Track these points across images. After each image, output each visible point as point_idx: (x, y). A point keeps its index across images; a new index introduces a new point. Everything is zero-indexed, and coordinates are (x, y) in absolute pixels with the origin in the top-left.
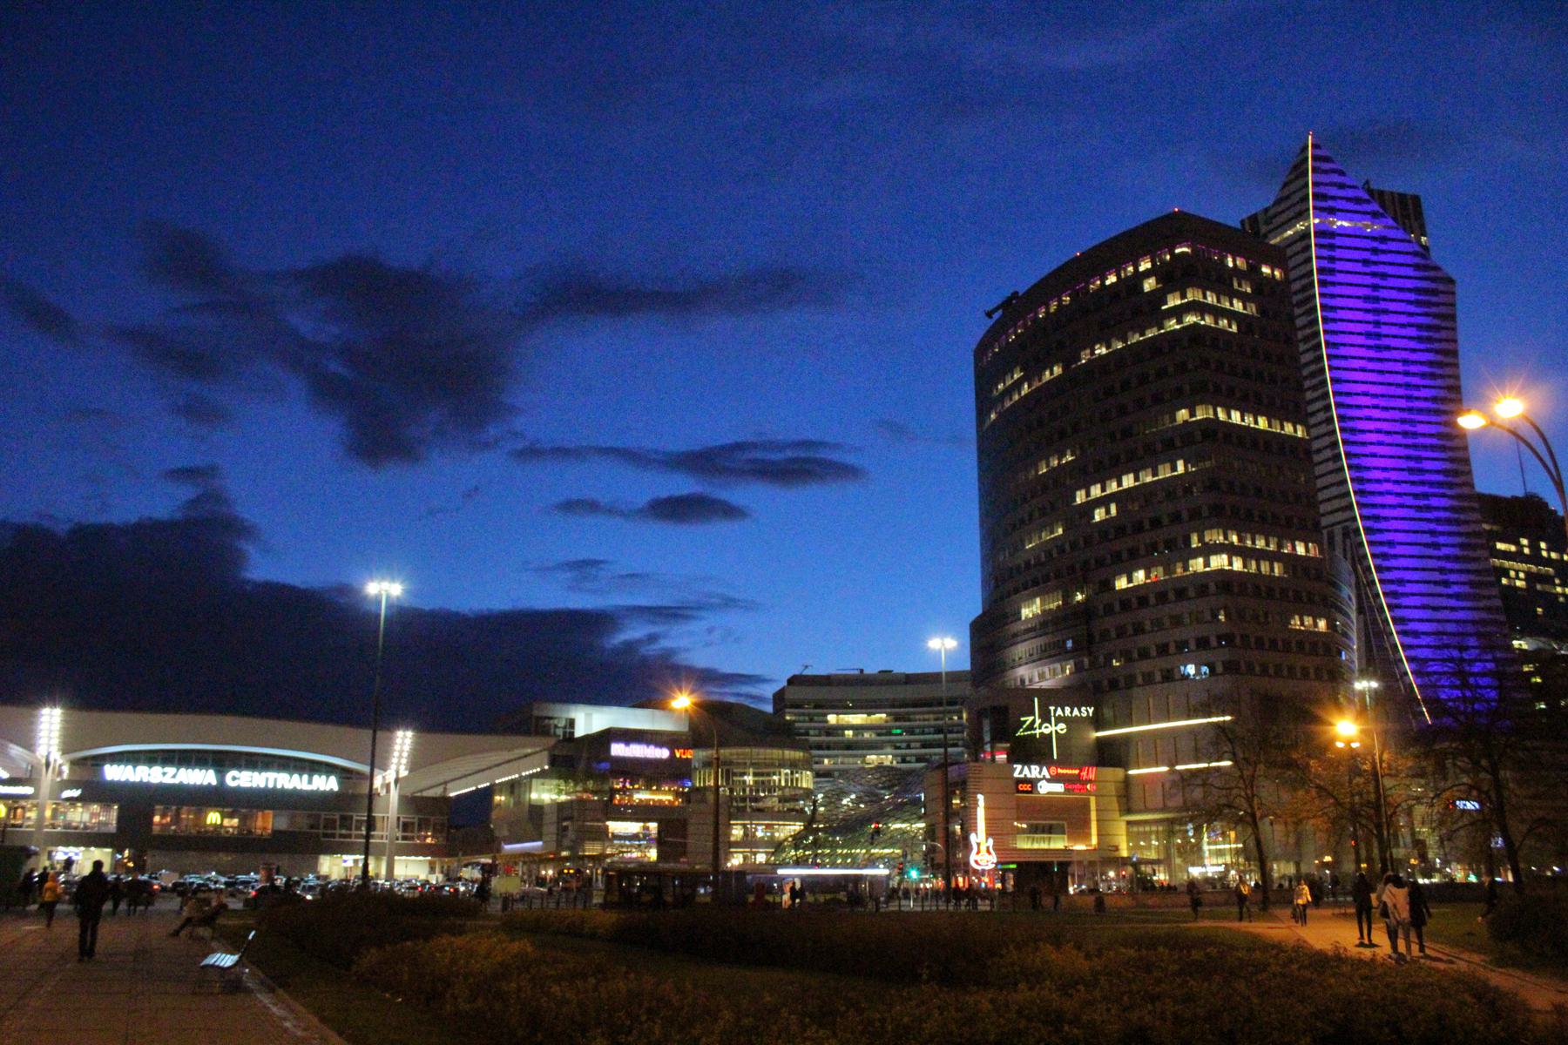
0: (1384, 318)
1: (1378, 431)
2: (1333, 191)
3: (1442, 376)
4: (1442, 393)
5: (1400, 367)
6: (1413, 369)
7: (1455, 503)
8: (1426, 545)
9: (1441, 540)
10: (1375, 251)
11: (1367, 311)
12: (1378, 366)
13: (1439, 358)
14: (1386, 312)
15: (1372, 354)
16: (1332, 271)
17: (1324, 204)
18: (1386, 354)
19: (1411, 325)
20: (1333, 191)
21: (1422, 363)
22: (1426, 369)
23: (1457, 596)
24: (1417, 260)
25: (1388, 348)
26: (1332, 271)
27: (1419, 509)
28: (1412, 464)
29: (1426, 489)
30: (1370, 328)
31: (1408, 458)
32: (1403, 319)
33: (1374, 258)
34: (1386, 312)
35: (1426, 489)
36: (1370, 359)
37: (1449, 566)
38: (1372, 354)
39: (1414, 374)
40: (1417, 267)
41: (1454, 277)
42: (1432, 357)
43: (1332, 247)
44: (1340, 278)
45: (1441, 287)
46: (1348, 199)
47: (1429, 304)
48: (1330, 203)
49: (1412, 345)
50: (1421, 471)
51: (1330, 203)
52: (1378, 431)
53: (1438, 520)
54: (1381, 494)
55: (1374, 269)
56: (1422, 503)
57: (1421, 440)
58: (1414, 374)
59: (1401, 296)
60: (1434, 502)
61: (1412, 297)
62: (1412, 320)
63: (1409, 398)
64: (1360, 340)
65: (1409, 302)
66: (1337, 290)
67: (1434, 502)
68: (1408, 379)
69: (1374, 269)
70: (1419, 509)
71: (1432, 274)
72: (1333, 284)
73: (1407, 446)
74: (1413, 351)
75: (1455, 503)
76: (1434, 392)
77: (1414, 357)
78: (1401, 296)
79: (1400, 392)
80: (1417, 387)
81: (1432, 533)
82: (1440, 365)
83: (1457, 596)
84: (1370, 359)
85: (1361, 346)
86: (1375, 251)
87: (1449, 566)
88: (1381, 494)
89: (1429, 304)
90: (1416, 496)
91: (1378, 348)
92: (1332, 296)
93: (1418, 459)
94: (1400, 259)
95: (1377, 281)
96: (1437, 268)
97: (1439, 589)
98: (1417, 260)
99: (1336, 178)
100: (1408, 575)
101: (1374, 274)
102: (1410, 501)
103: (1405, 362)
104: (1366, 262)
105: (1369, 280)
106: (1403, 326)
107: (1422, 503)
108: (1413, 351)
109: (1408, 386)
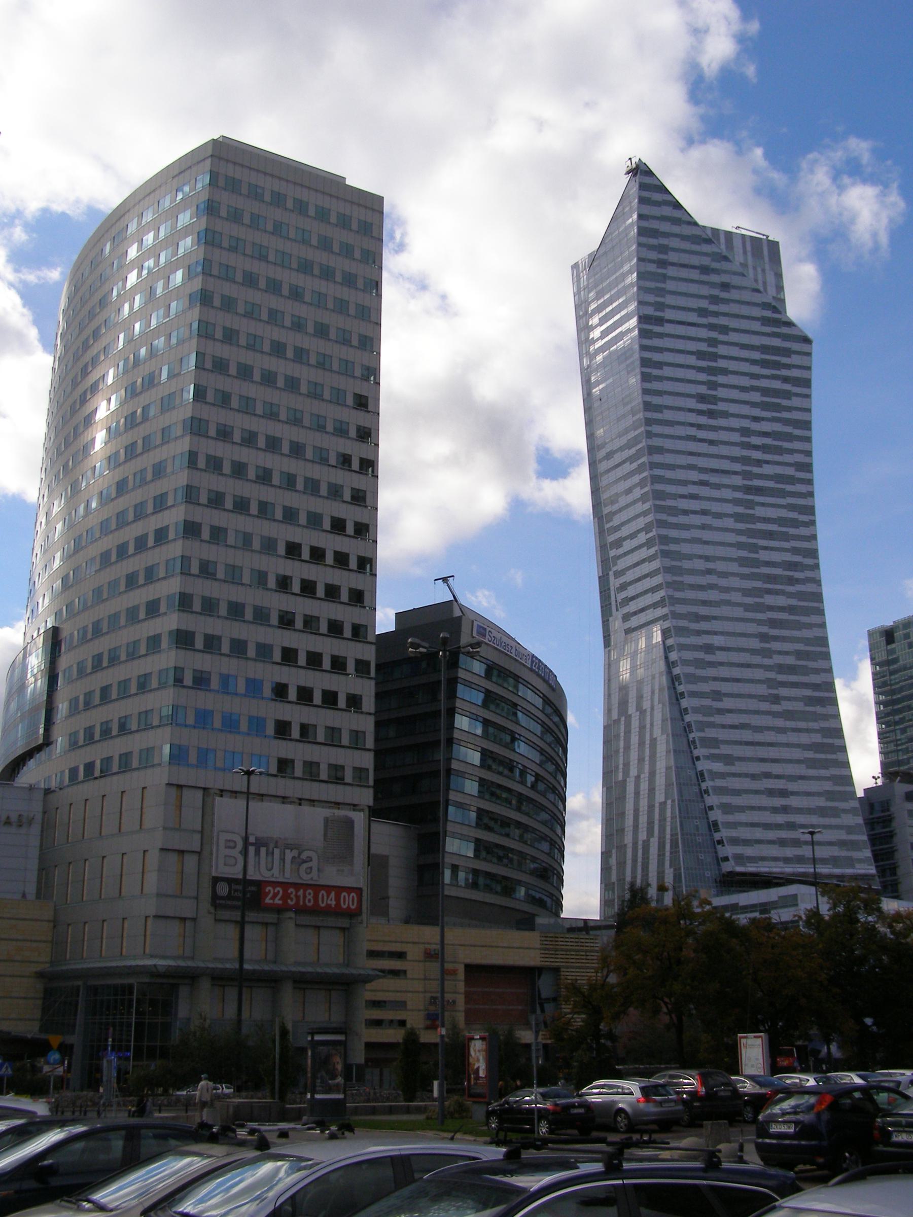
0: (721, 379)
1: (704, 512)
2: (665, 227)
3: (791, 452)
4: (790, 471)
5: (736, 437)
6: (756, 440)
7: (793, 602)
8: (753, 652)
9: (776, 646)
10: (715, 300)
11: (700, 369)
12: (711, 435)
13: (788, 429)
14: (725, 372)
15: (703, 420)
16: (660, 321)
17: (653, 241)
18: (722, 422)
20: (665, 227)
21: (766, 434)
22: (768, 441)
23: (789, 715)
24: (768, 314)
25: (725, 414)
26: (660, 321)
27: (747, 608)
29: (758, 584)
30: (703, 389)
31: (740, 546)
32: (745, 382)
33: (713, 308)
34: (725, 372)
35: (758, 584)
36: (700, 427)
37: (781, 678)
39: (756, 447)
40: (765, 321)
41: (810, 335)
42: (778, 427)
43: (662, 292)
44: (668, 328)
45: (796, 346)
46: (684, 238)
47: (777, 365)
48: (663, 241)
49: (757, 412)
50: (757, 563)
51: (663, 241)
52: (704, 512)
53: (773, 623)
54: (701, 588)
55: (712, 320)
56: (749, 600)
57: (760, 526)
58: (756, 447)
59: (745, 354)
60: (769, 600)
61: (756, 355)
62: (755, 383)
63: (747, 475)
64: (692, 403)
65: (754, 362)
66: (656, 342)
67: (769, 600)
68: (745, 453)
69: (712, 320)
70: (747, 608)
71: (785, 330)
72: (661, 335)
73: (740, 532)
74: (756, 419)
75: (793, 602)
76: (779, 470)
77: (755, 426)
78: (745, 354)
79: (737, 467)
80: (759, 463)
81: (764, 637)
82: (790, 438)
83: (789, 715)
84: (700, 427)
85: (691, 410)
86: (715, 300)
87: (781, 678)
88: (701, 588)
89: (777, 365)
90: (746, 592)
91: (711, 414)
92: (660, 350)
93: (755, 548)
94: (745, 310)
95: (714, 335)
96: (790, 324)
97: (764, 706)
98: (768, 314)
99: (667, 211)
100: (725, 687)
101: (712, 327)
102: (736, 597)
103: (745, 432)
104: (702, 312)
105: (703, 333)
106: (743, 389)
107: (749, 600)
108: (756, 419)
109: (745, 460)
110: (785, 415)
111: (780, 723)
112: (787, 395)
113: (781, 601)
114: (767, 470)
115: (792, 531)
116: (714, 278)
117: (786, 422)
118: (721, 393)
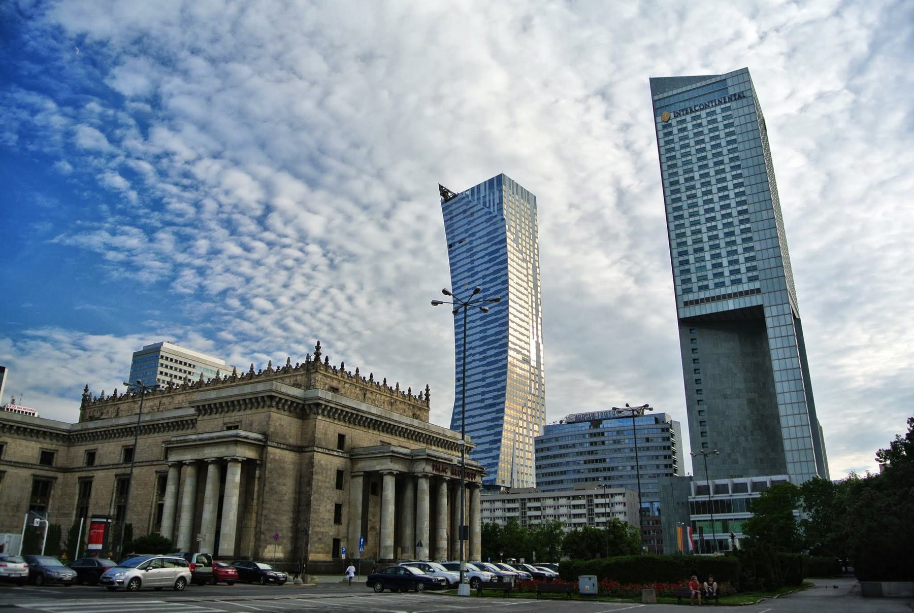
7: (497, 351)
18: (476, 277)
19: (486, 255)
22: (492, 277)
28: (482, 335)
38: (470, 280)
42: (496, 268)
55: (470, 232)
61: (485, 239)
69: (470, 232)
70: (480, 360)
74: (487, 269)
75: (497, 351)
84: (469, 283)
90: (481, 353)
108: (487, 269)
110: (498, 261)
111: (483, 411)
112: (497, 250)
113: (493, 352)
114: (492, 291)
115: (499, 316)
116: (468, 213)
117: (497, 264)
118: (476, 263)
